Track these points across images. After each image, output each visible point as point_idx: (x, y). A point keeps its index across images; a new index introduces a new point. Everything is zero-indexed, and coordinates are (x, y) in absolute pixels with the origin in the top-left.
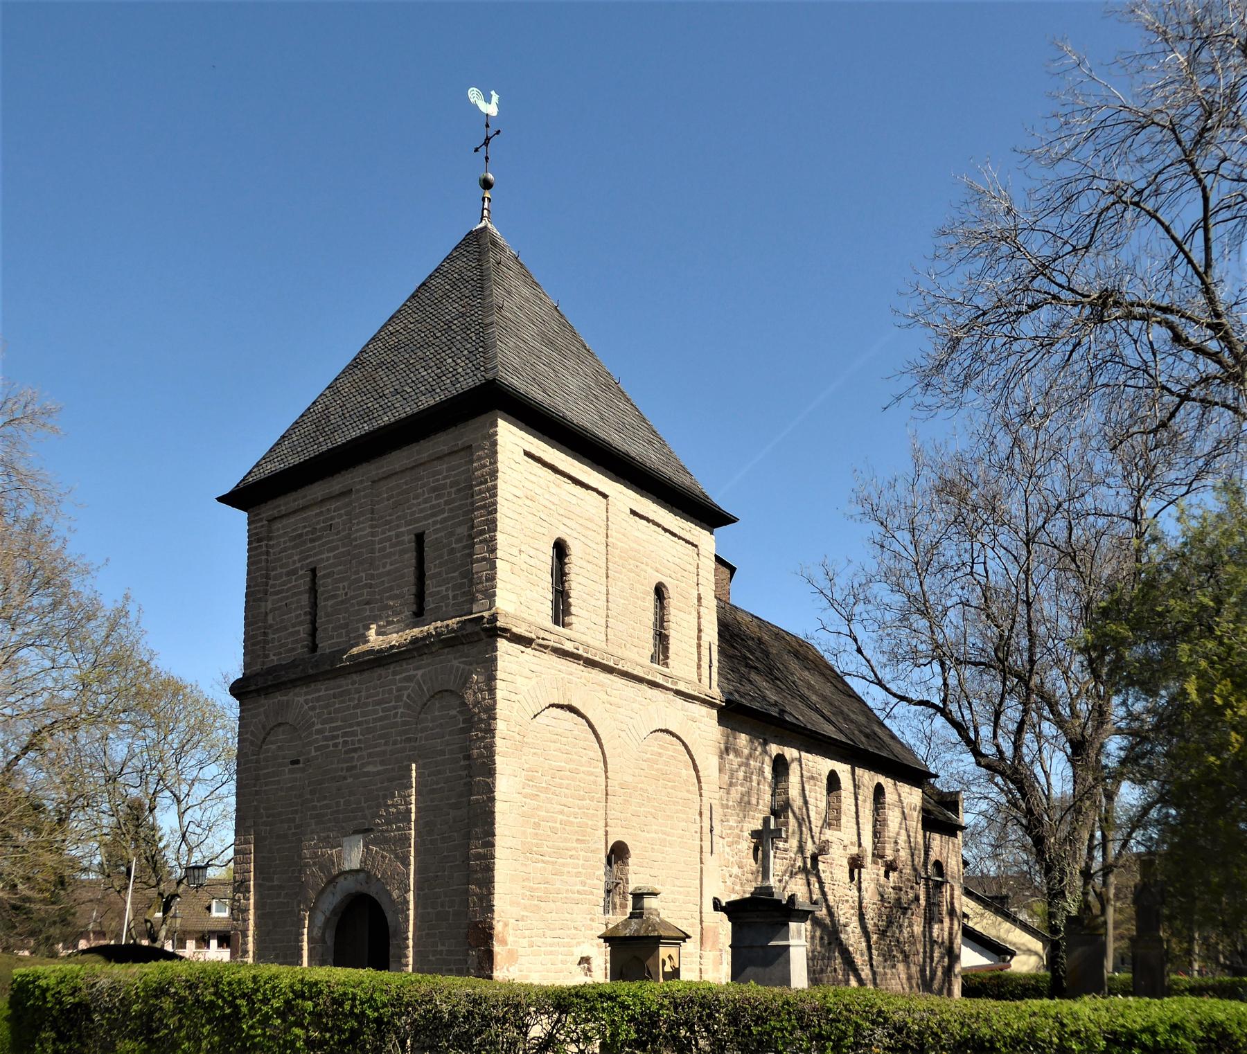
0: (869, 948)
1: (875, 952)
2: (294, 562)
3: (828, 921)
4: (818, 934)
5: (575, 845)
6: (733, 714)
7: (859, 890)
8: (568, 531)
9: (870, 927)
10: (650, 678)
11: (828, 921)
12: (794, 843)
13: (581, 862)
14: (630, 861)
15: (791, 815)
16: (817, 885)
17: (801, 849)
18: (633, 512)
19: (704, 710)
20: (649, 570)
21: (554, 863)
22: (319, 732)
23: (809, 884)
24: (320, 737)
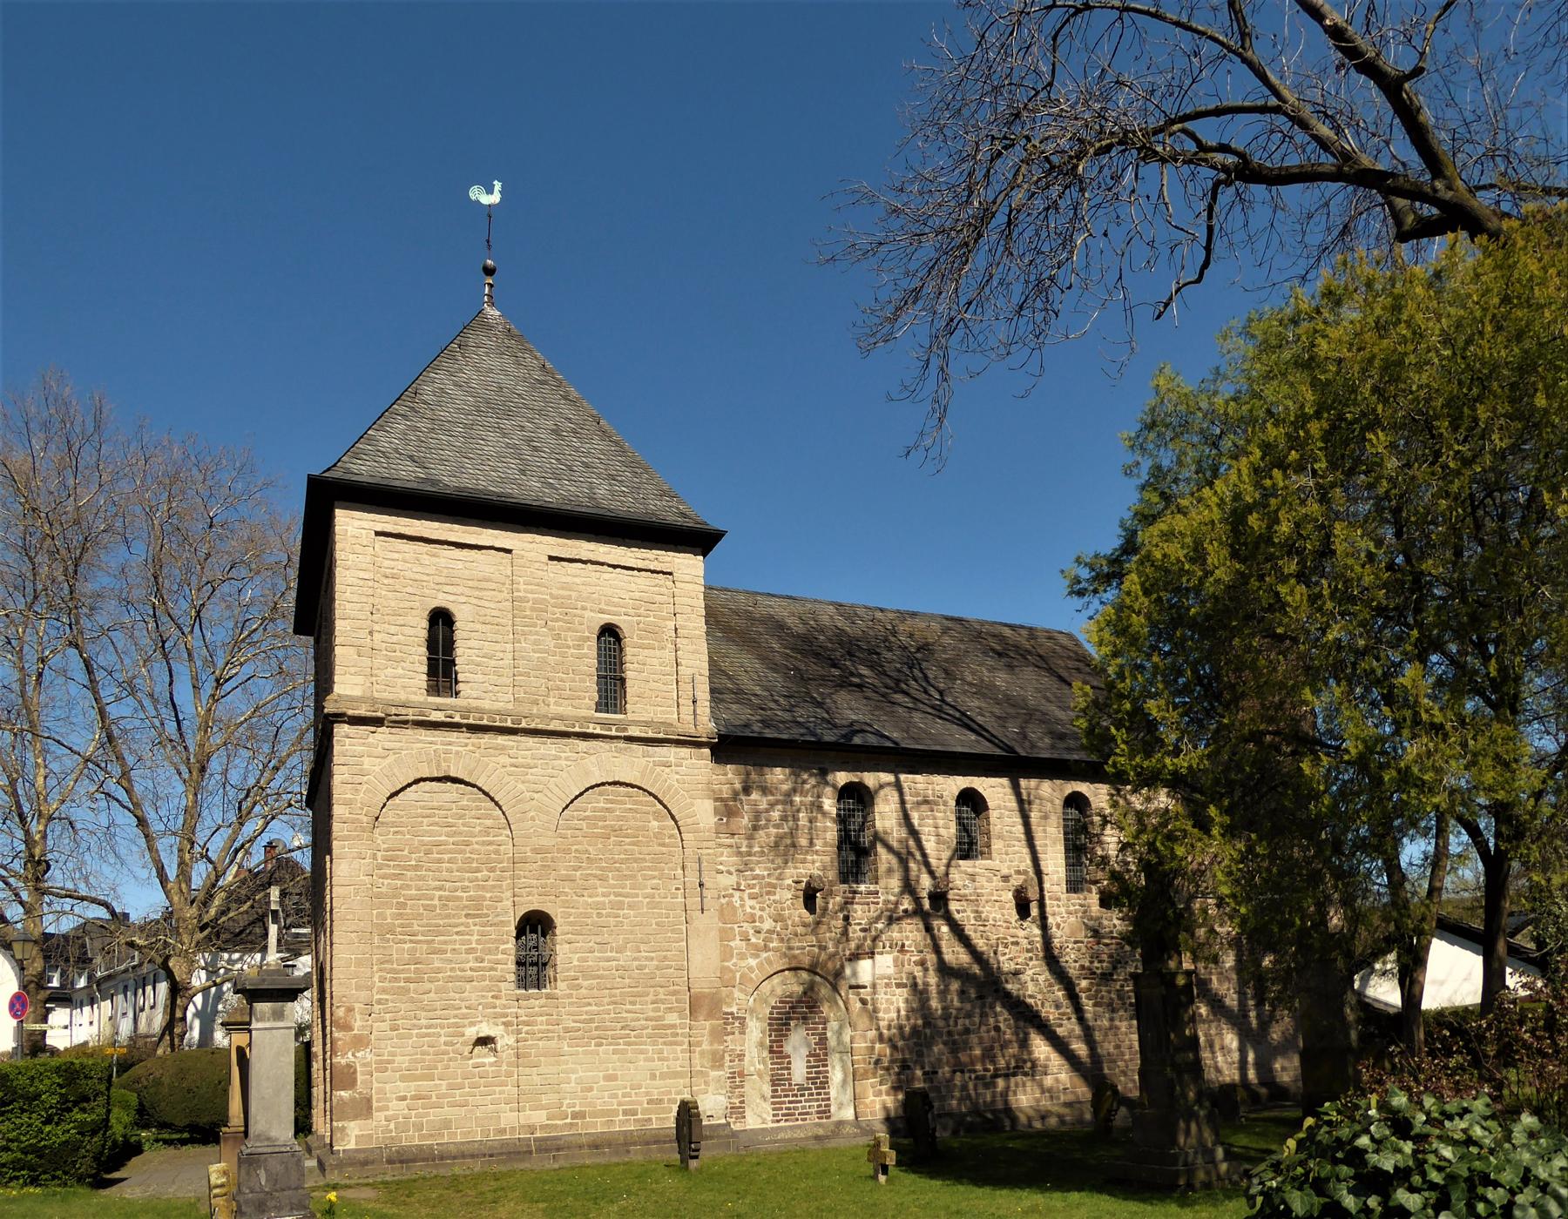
0: (1073, 997)
1: (1088, 1006)
3: (976, 969)
4: (955, 986)
5: (463, 920)
6: (726, 748)
7: (1044, 927)
8: (452, 598)
9: (1073, 972)
10: (577, 729)
11: (976, 969)
12: (895, 883)
13: (476, 937)
14: (558, 931)
15: (880, 849)
16: (945, 929)
17: (909, 887)
18: (551, 558)
19: (684, 751)
20: (587, 614)
21: (427, 942)
23: (928, 929)
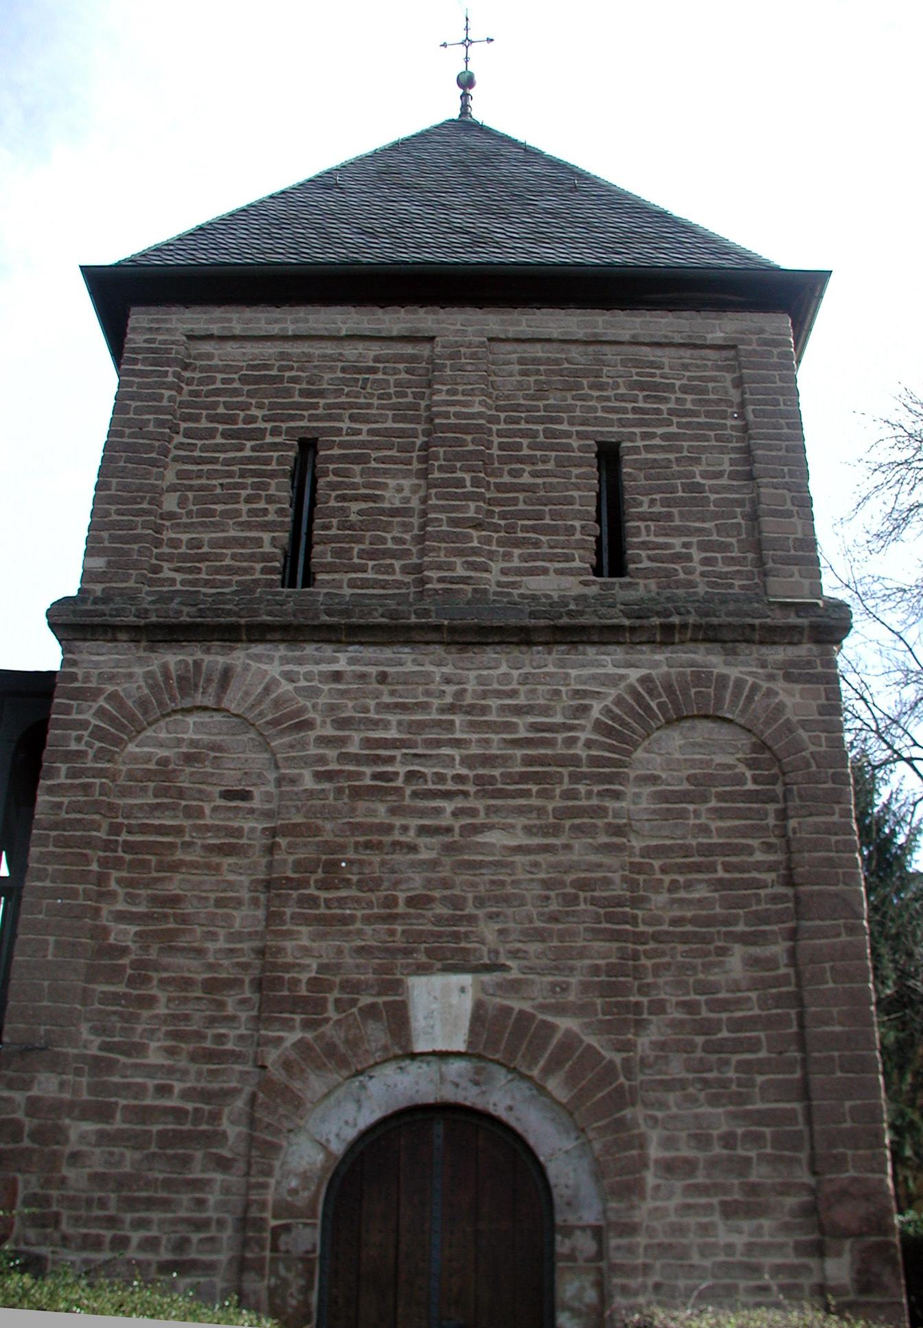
2: (252, 419)
22: (323, 741)
24: (331, 753)
